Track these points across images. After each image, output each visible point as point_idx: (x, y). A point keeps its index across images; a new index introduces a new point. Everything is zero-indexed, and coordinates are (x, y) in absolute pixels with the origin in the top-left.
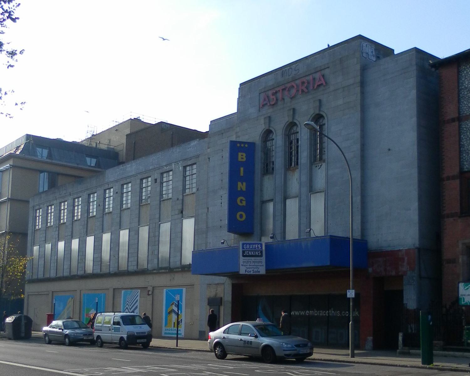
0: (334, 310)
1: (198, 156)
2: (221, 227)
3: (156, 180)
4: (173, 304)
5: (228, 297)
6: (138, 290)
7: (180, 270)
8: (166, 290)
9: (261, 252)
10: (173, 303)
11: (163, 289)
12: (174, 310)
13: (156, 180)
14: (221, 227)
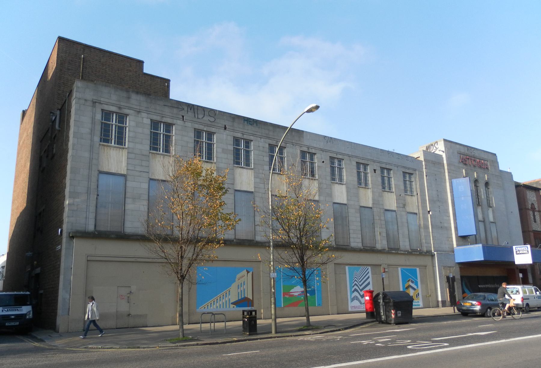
0: (497, 284)
1: (415, 170)
2: (441, 227)
3: (375, 170)
4: (409, 281)
5: (458, 277)
6: (368, 267)
7: (418, 253)
8: (401, 269)
9: (528, 251)
10: (409, 280)
11: (398, 268)
12: (410, 285)
13: (375, 170)
14: (441, 227)
